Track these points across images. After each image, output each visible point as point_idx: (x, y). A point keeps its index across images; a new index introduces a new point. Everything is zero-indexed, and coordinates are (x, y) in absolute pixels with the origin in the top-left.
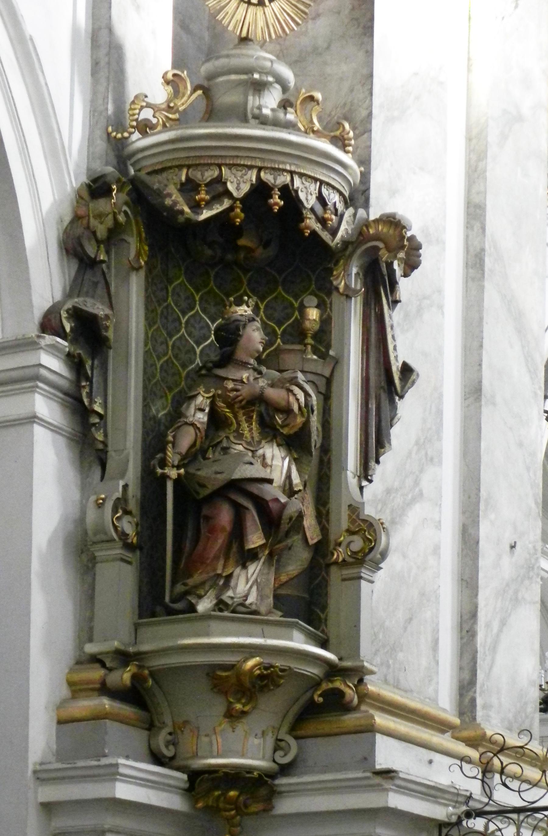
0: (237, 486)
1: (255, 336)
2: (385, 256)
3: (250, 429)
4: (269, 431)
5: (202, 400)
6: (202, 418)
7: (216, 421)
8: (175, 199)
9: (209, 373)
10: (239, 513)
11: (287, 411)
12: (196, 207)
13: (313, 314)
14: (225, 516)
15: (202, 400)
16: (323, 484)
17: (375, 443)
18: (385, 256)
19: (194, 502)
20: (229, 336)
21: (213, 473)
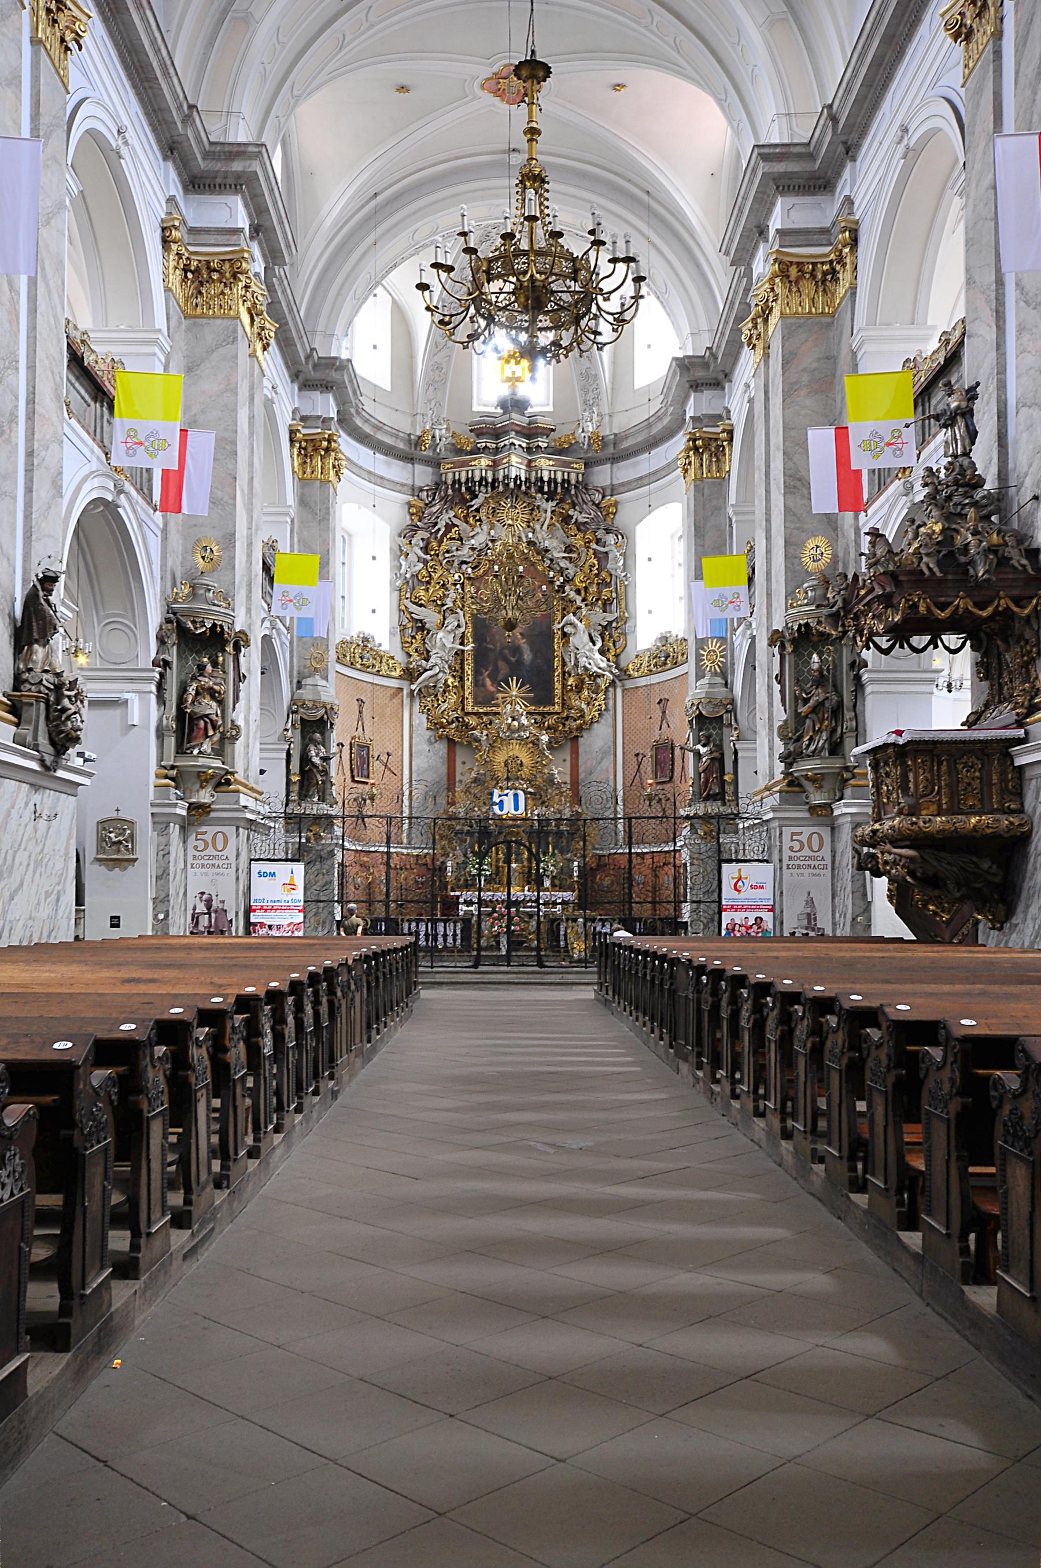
0: (207, 716)
1: (209, 668)
2: (241, 641)
3: (208, 697)
4: (213, 698)
5: (194, 686)
6: (193, 693)
7: (197, 693)
8: (190, 625)
9: (194, 678)
10: (206, 722)
11: (219, 693)
12: (196, 628)
13: (221, 659)
14: (202, 723)
15: (194, 686)
16: (223, 712)
17: (236, 699)
18: (241, 641)
19: (194, 718)
20: (201, 668)
21: (199, 710)
